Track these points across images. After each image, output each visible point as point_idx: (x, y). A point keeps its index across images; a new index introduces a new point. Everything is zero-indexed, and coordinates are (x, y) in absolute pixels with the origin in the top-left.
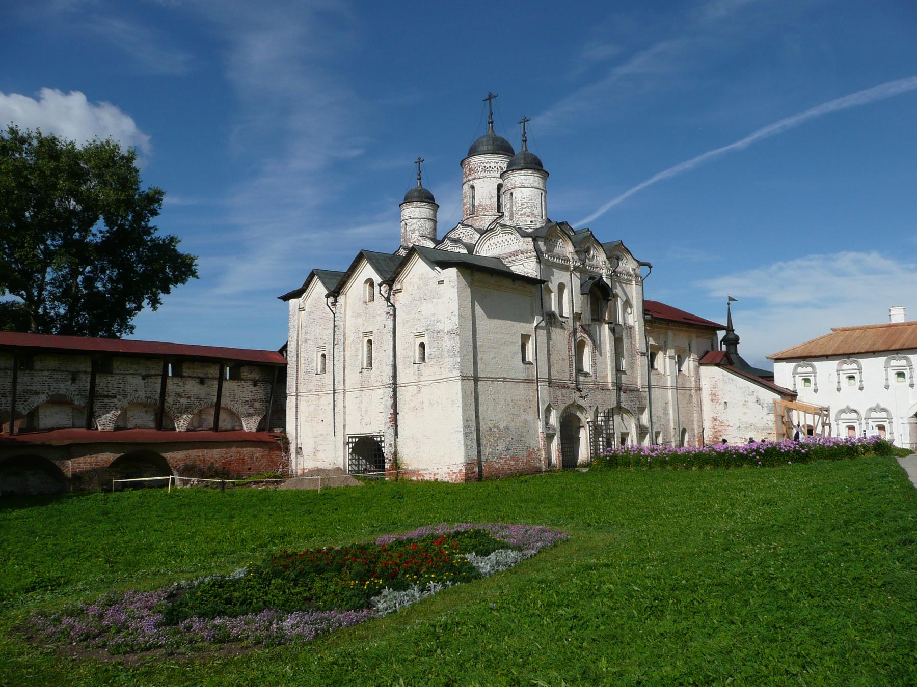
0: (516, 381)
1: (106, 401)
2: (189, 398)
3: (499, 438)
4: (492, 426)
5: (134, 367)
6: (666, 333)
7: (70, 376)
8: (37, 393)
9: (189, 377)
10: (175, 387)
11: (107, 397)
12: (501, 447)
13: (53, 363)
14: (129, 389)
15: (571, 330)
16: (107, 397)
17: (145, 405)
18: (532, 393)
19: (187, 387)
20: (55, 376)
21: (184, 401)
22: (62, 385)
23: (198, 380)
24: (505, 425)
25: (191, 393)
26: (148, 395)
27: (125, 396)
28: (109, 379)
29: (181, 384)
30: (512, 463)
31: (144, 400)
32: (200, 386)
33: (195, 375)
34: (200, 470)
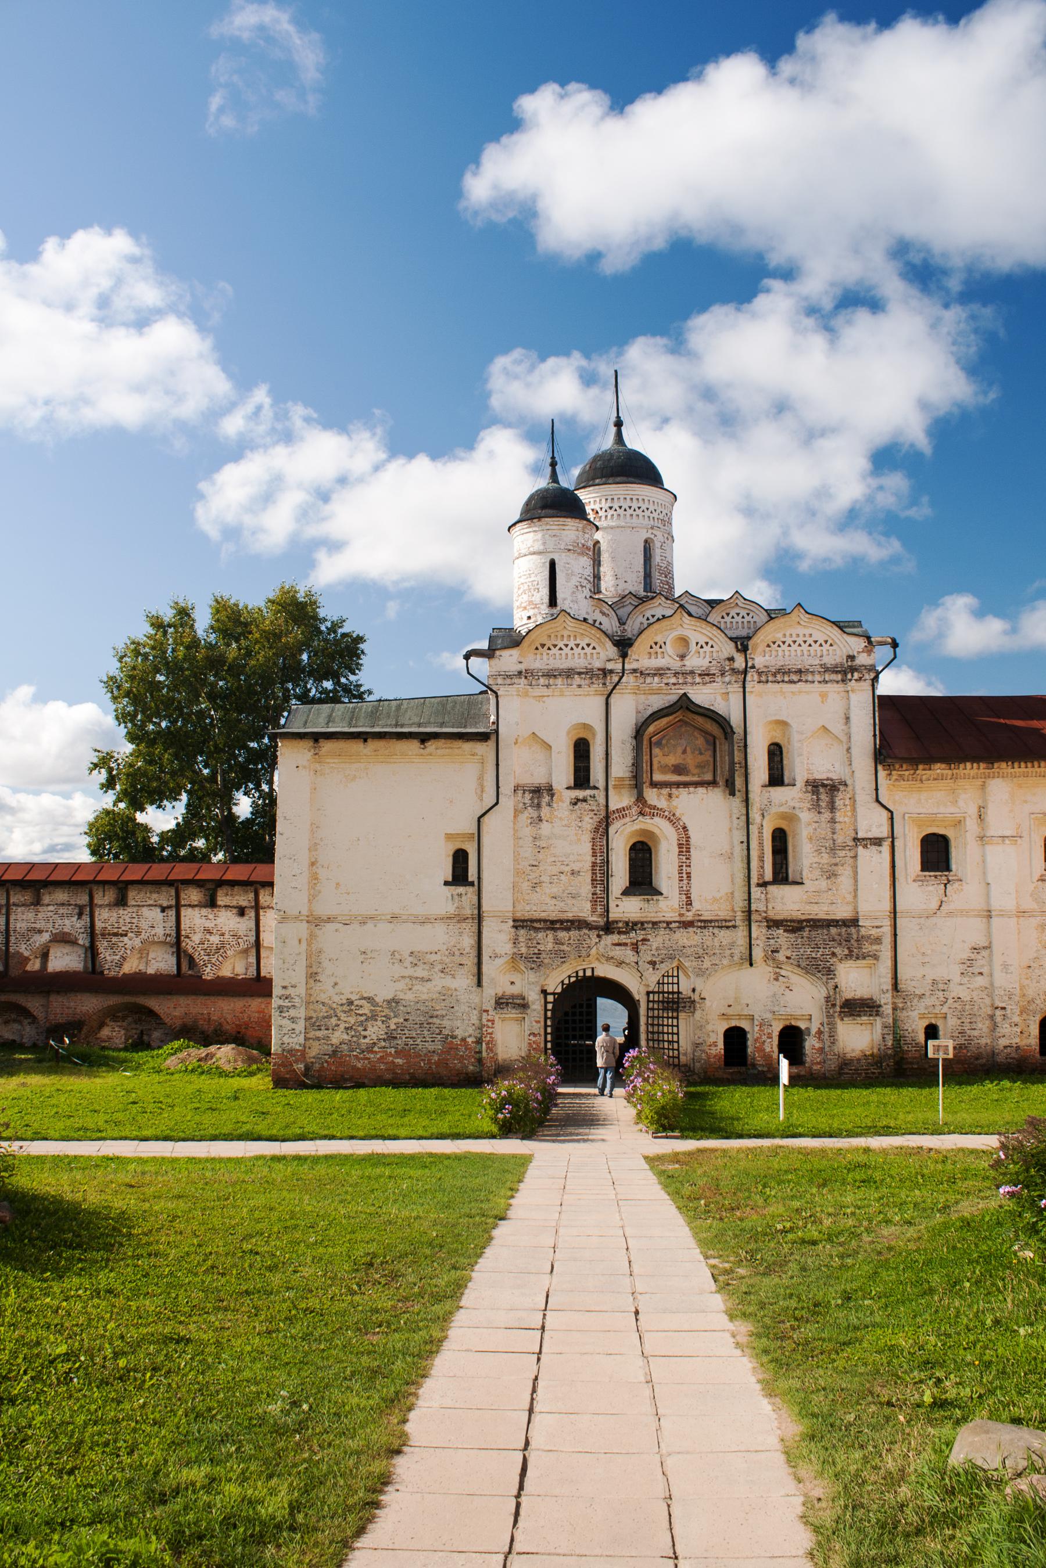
0: (425, 921)
1: (114, 939)
2: (223, 935)
3: (374, 1017)
4: (353, 997)
5: (155, 896)
6: (983, 786)
7: (77, 911)
8: (40, 932)
9: (226, 906)
10: (204, 920)
11: (116, 934)
12: (375, 1031)
13: (61, 896)
14: (144, 925)
15: (603, 814)
16: (116, 934)
17: (164, 943)
18: (468, 942)
19: (219, 920)
20: (61, 911)
21: (215, 939)
22: (67, 922)
23: (235, 911)
24: (390, 997)
25: (225, 929)
26: (168, 932)
27: (138, 933)
28: (121, 912)
29: (211, 916)
30: (399, 1061)
31: (162, 939)
32: (238, 919)
33: (234, 903)
34: (202, 1033)
